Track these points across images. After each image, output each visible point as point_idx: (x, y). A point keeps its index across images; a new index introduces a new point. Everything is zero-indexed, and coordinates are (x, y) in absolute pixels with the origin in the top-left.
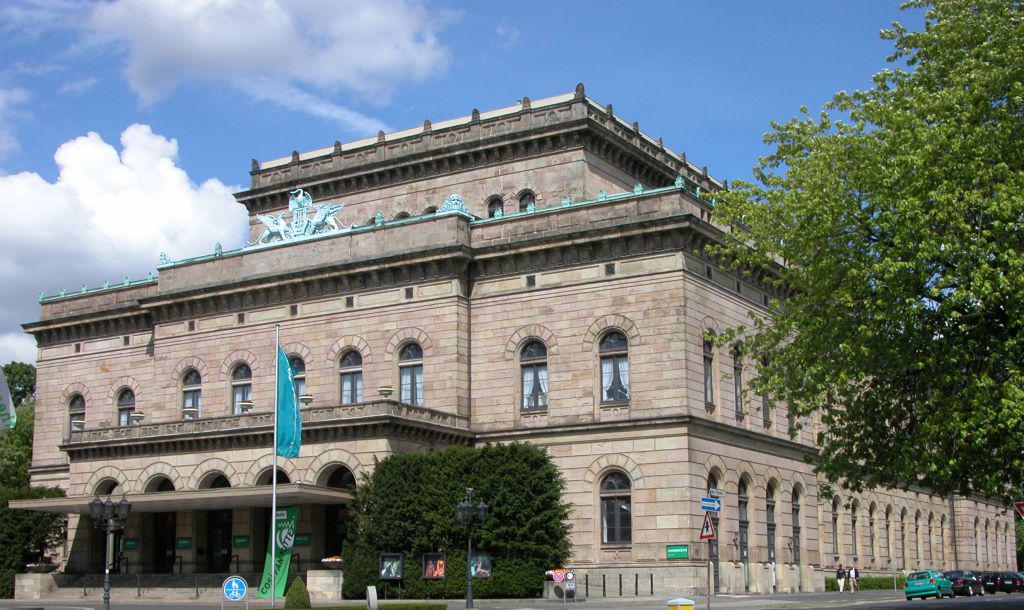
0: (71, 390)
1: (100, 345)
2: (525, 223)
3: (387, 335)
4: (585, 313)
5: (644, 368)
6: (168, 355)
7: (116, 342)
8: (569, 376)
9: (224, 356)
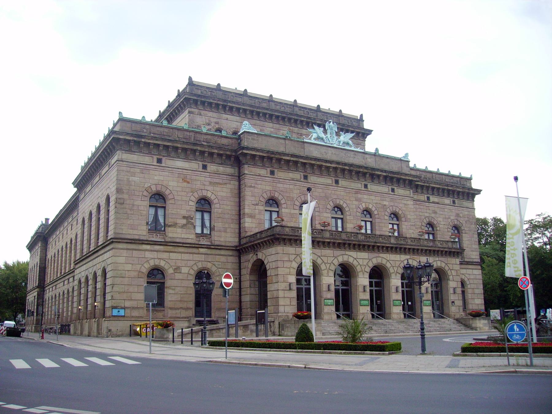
0: (154, 189)
1: (180, 163)
2: (424, 174)
3: (385, 207)
4: (447, 216)
6: (256, 186)
7: (195, 165)
9: (295, 196)
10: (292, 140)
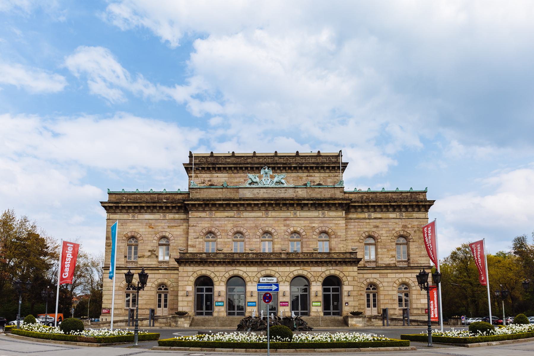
0: (129, 234)
5: (415, 250)
8: (386, 250)
10: (228, 188)
